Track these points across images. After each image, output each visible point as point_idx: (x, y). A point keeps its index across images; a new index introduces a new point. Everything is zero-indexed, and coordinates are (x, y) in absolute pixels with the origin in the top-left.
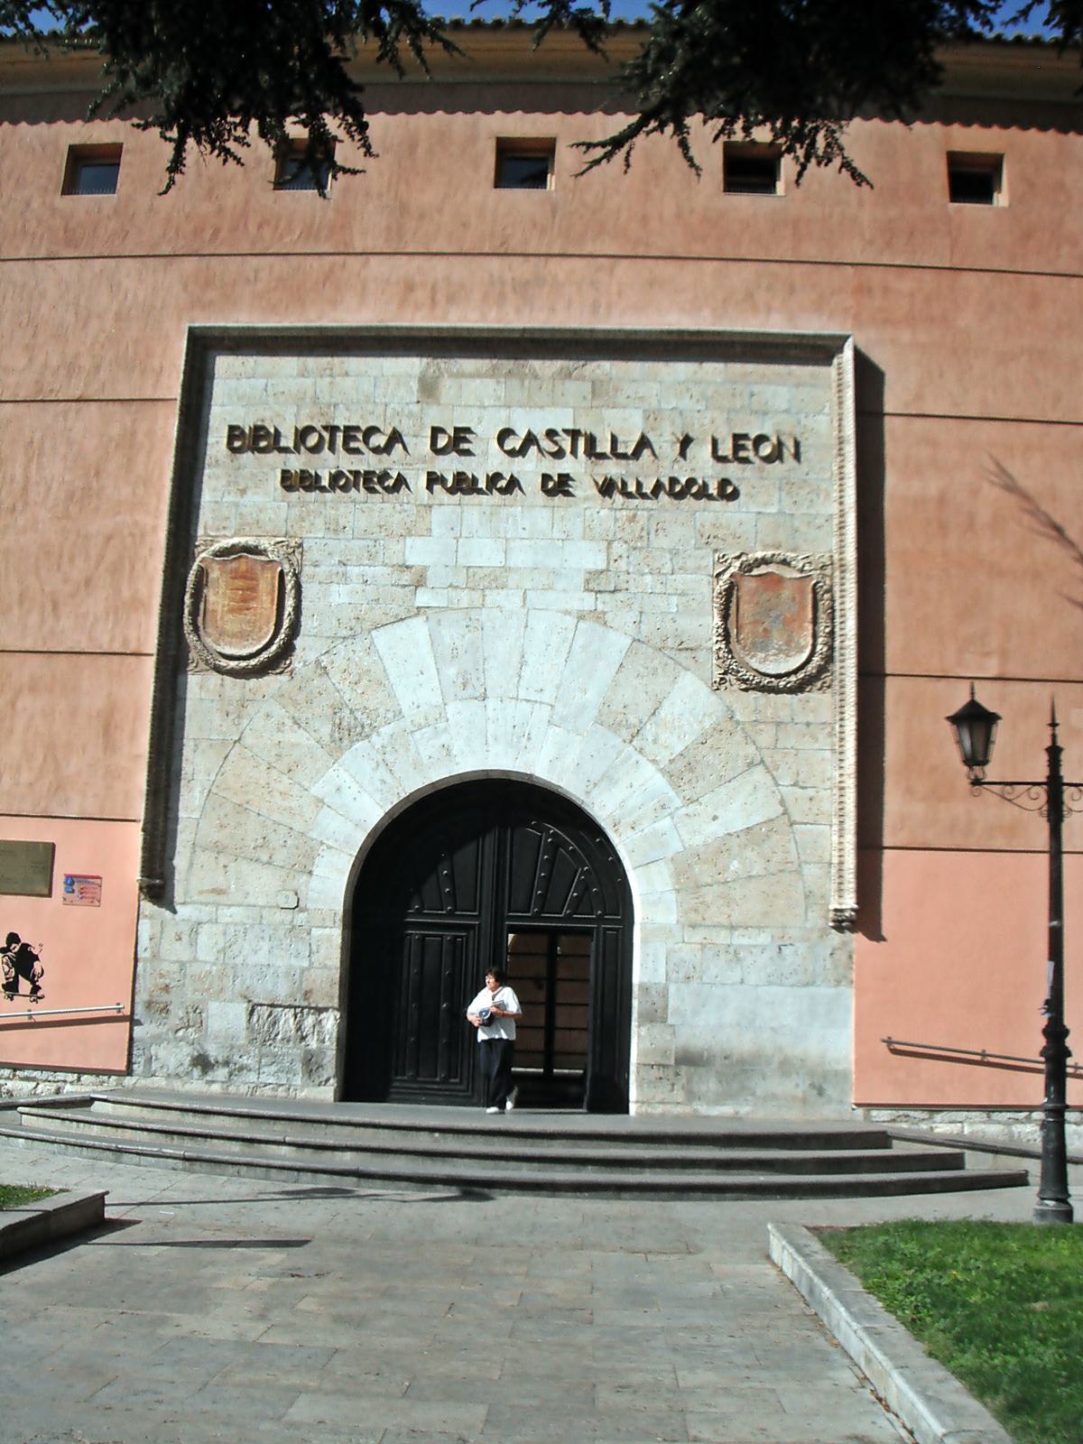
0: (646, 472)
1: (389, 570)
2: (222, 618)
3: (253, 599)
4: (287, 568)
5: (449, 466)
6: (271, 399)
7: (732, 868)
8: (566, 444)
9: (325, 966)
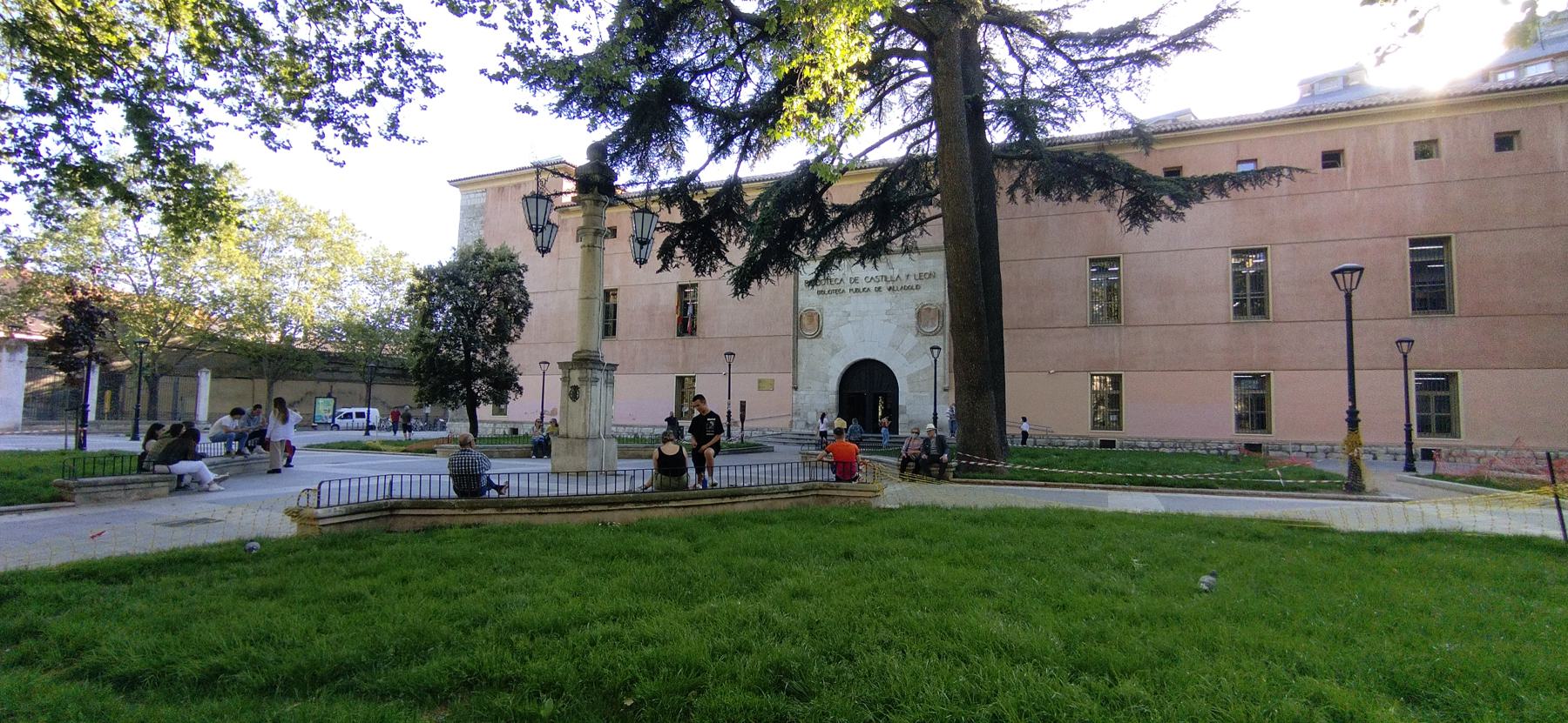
0: (898, 284)
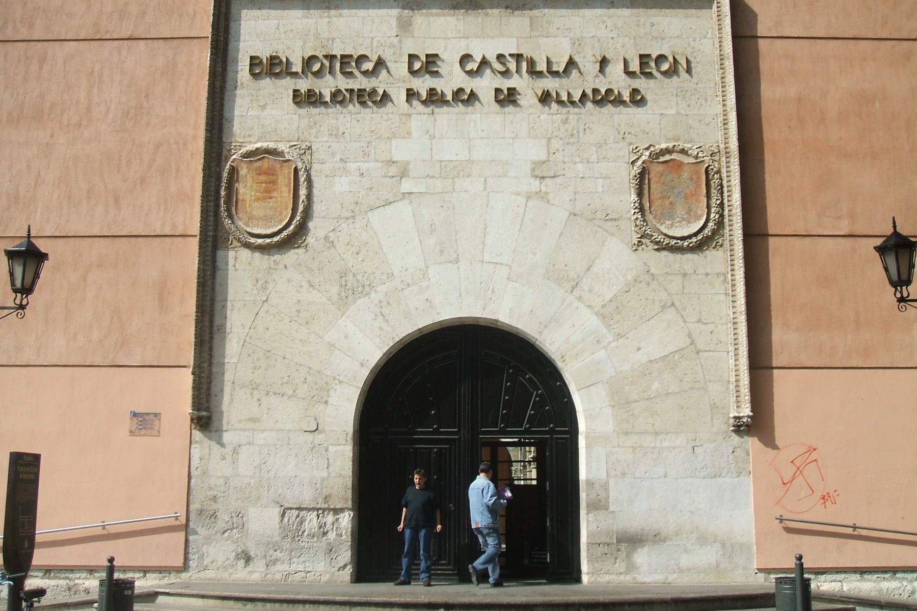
0: (574, 86)
1: (380, 165)
2: (250, 206)
3: (275, 190)
4: (300, 165)
5: (423, 85)
6: (282, 36)
7: (654, 388)
8: (512, 66)
9: (341, 475)
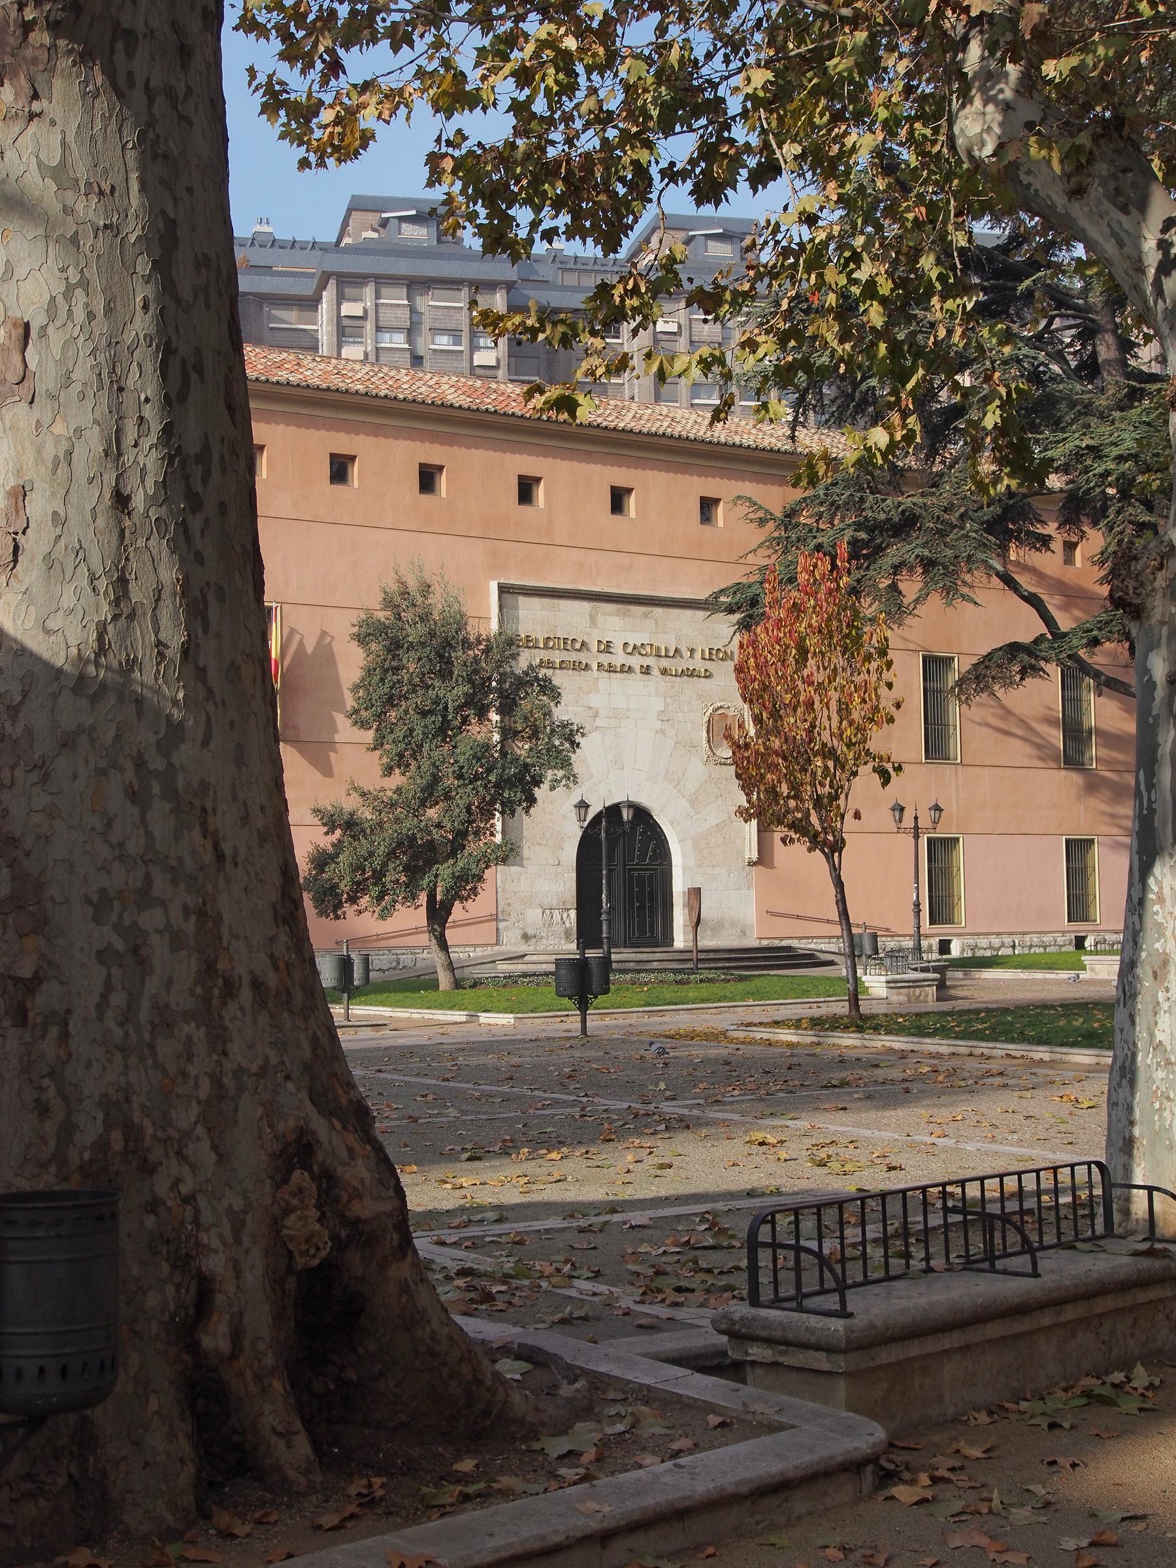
5: (605, 659)
